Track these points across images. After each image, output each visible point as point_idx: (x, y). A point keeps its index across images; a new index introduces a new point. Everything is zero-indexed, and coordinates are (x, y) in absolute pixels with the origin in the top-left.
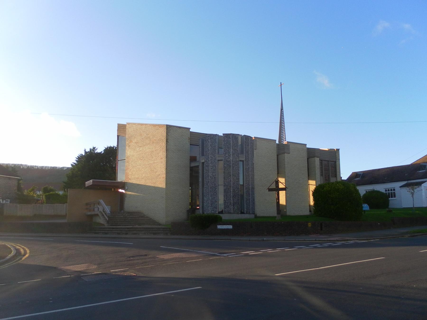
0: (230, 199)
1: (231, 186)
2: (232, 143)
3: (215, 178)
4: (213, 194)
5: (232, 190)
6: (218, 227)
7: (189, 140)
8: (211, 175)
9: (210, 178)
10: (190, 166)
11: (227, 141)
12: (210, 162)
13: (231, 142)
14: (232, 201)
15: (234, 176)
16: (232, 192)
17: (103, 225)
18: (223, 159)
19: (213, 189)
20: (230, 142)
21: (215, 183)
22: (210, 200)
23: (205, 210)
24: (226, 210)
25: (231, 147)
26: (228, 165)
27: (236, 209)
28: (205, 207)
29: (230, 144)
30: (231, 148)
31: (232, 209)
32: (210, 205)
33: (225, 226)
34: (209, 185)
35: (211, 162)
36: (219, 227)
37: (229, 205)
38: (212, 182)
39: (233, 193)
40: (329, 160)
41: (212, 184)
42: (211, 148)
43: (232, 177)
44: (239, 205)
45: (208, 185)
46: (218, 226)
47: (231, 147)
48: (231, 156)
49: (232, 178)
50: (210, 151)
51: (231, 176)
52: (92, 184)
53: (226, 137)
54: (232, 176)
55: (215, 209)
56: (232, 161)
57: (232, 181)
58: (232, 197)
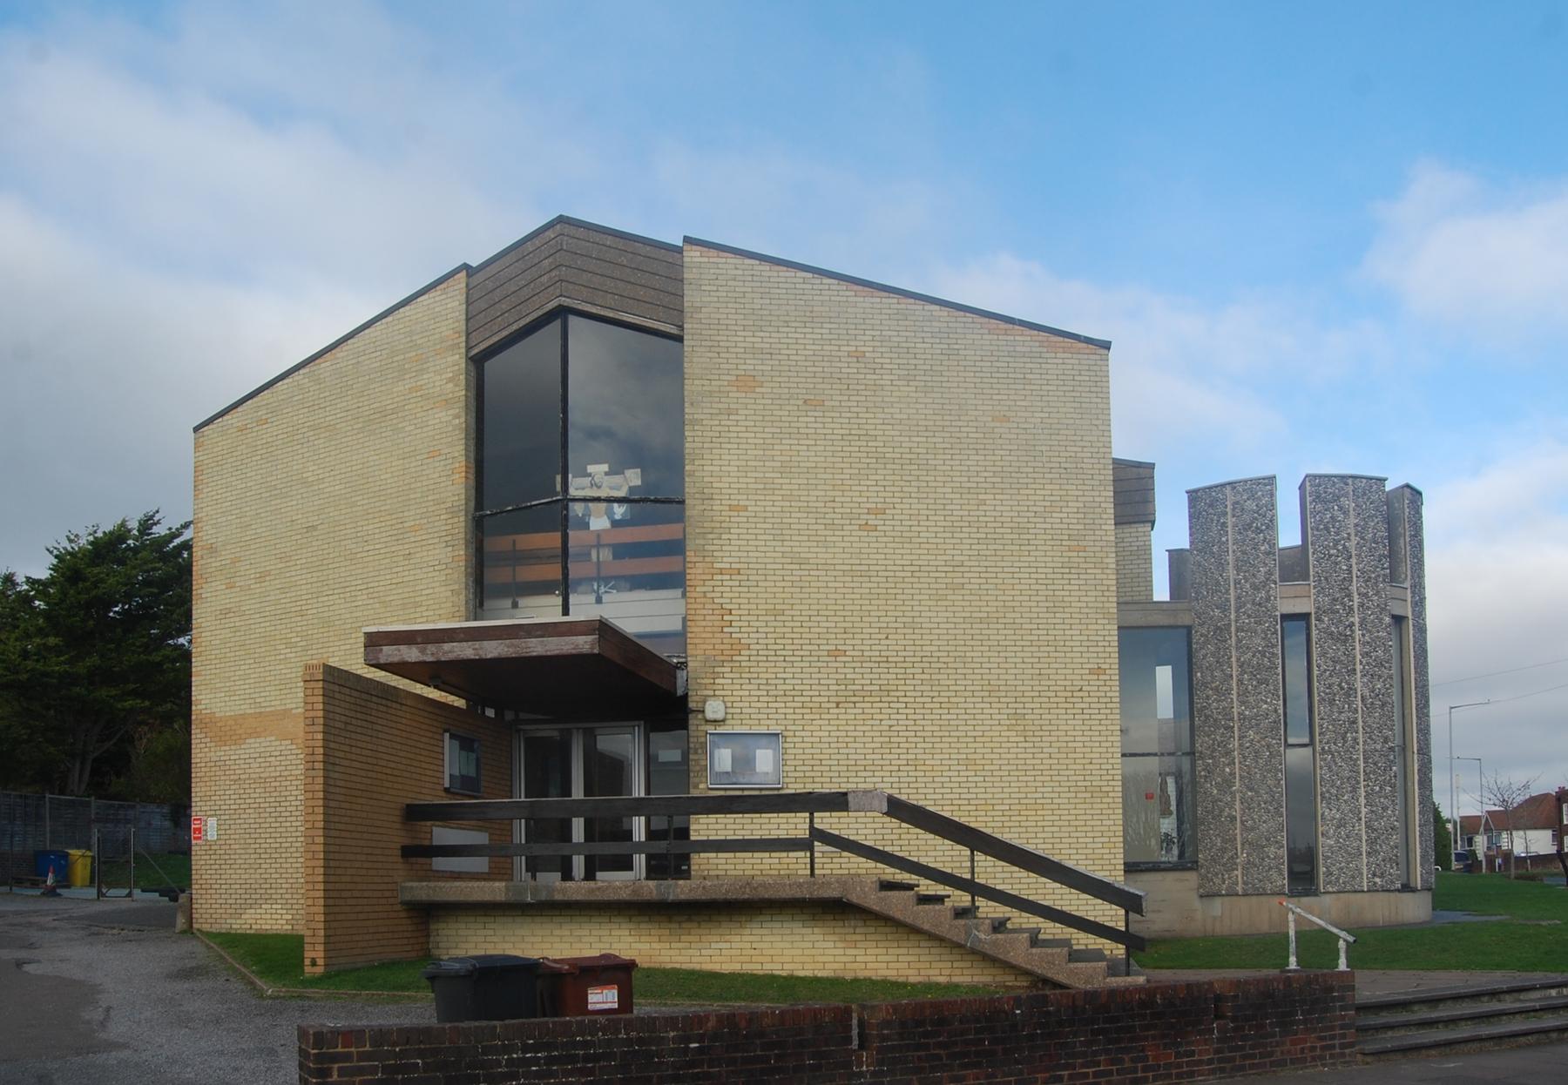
3: (1383, 705)
4: (1378, 788)
12: (1356, 620)
19: (1375, 764)
28: (1329, 858)
32: (1364, 848)
34: (1355, 740)
35: (1363, 622)
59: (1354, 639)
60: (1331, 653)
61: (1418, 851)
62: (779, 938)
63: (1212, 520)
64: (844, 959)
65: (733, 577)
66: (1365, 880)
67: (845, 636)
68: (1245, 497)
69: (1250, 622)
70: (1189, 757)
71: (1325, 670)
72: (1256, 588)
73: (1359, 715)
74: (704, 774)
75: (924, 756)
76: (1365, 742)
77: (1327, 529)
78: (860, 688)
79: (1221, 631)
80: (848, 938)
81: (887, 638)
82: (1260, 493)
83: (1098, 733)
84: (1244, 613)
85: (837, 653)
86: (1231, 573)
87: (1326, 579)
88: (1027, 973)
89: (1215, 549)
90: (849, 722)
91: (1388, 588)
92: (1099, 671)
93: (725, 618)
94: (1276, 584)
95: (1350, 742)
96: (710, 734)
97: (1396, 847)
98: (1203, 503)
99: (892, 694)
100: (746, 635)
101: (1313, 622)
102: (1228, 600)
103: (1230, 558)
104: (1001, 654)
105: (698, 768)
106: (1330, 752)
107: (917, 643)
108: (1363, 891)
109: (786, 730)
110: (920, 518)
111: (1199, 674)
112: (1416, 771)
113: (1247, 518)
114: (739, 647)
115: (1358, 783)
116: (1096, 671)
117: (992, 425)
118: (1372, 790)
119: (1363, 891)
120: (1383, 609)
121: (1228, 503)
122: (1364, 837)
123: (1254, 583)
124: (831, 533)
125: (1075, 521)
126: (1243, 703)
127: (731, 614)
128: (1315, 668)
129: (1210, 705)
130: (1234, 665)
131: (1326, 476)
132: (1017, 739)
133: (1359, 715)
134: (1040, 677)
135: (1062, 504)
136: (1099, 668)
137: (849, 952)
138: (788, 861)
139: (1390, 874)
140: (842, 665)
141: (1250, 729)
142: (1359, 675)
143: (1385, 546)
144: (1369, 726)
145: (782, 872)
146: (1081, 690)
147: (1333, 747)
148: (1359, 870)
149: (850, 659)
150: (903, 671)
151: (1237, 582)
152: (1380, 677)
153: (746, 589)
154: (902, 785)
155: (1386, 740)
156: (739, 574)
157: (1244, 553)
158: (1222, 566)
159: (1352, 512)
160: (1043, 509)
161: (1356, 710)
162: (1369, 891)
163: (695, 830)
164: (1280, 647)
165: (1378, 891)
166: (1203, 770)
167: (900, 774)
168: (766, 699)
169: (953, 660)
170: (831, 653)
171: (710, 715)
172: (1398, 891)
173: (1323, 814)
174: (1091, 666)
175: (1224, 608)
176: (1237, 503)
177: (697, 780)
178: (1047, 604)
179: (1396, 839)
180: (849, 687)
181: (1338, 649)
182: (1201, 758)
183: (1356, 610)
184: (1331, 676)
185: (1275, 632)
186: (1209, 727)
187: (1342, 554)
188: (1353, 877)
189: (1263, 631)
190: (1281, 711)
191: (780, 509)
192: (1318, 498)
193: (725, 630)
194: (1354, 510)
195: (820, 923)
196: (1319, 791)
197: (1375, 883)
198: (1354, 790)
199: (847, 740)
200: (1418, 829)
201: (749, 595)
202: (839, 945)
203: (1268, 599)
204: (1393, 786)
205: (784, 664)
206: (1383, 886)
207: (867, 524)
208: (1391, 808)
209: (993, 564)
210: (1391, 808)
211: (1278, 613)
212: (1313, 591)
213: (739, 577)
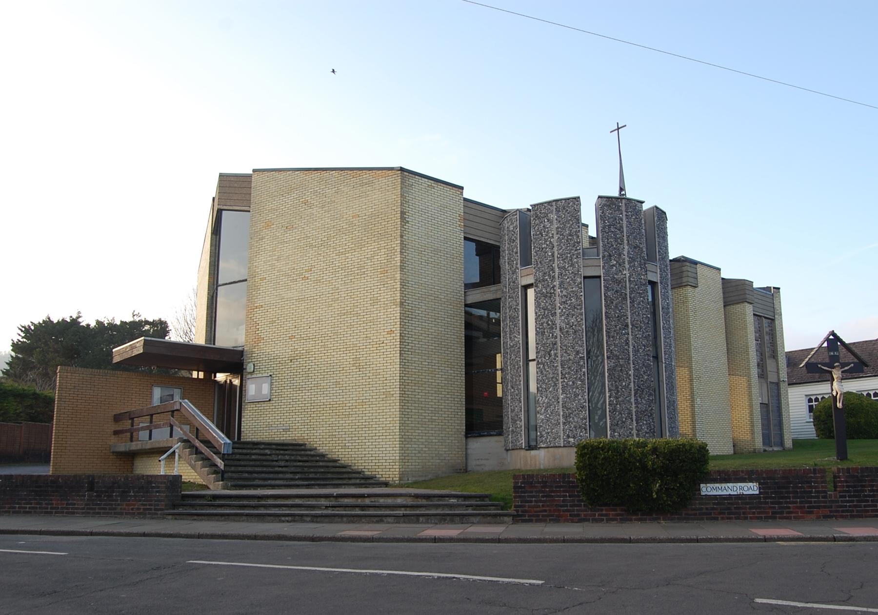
0: (627, 399)
1: (629, 359)
2: (627, 227)
5: (631, 372)
6: (704, 489)
7: (462, 224)
9: (557, 332)
10: (465, 300)
11: (612, 219)
12: (557, 283)
13: (625, 222)
14: (634, 405)
15: (637, 327)
16: (632, 378)
17: (206, 487)
18: (601, 272)
19: (569, 368)
20: (619, 223)
21: (577, 348)
22: (561, 403)
23: (542, 436)
24: (616, 434)
25: (625, 238)
26: (616, 291)
27: (646, 433)
28: (541, 426)
29: (622, 227)
30: (626, 242)
31: (634, 432)
32: (562, 420)
33: (730, 485)
34: (556, 355)
35: (561, 284)
36: (708, 489)
37: (624, 420)
38: (565, 346)
39: (634, 382)
40: (761, 314)
41: (566, 352)
43: (630, 330)
44: (653, 419)
45: (550, 356)
46: (702, 485)
47: (625, 238)
48: (627, 266)
49: (632, 332)
50: (555, 249)
51: (627, 326)
52: (142, 352)
53: (609, 206)
54: (630, 326)
56: (630, 281)
57: (631, 343)
58: (633, 392)
59: (555, 294)
73: (558, 339)
75: (321, 382)
77: (541, 234)
87: (541, 262)
97: (585, 419)
108: (561, 447)
115: (558, 380)
118: (567, 384)
119: (561, 447)
131: (540, 204)
133: (558, 339)
139: (581, 436)
142: (558, 315)
146: (383, 343)
147: (543, 359)
152: (573, 315)
155: (578, 353)
165: (571, 446)
167: (312, 391)
174: (388, 330)
178: (371, 302)
181: (547, 302)
184: (542, 318)
194: (557, 219)
198: (556, 385)
204: (582, 381)
206: (574, 443)
211: (520, 286)
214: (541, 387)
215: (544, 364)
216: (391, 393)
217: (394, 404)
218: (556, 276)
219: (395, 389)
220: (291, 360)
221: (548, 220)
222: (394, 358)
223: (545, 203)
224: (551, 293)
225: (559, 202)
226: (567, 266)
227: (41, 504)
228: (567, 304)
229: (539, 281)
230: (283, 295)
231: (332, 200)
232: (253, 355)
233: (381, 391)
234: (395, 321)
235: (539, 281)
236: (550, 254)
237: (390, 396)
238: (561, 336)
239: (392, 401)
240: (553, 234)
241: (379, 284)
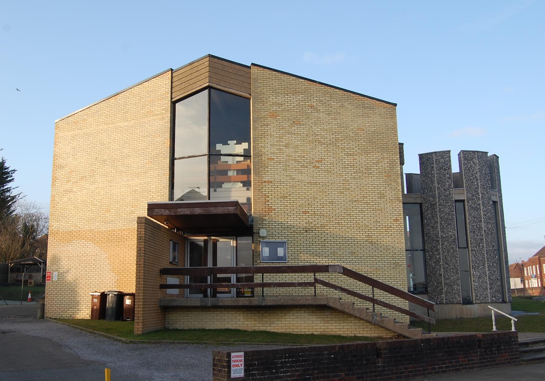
4: (492, 264)
8: (486, 229)
12: (481, 202)
19: (490, 255)
28: (476, 290)
32: (488, 286)
34: (483, 246)
38: (487, 241)
42: (480, 176)
50: (479, 181)
55: (498, 294)
59: (480, 209)
60: (473, 215)
61: (506, 288)
62: (300, 320)
63: (428, 165)
64: (324, 327)
65: (269, 184)
66: (489, 299)
67: (308, 206)
68: (440, 158)
69: (443, 203)
70: (422, 252)
71: (471, 221)
72: (445, 190)
74: (259, 257)
76: (486, 247)
78: (314, 225)
79: (433, 205)
80: (325, 319)
81: (323, 207)
82: (445, 157)
83: (397, 243)
84: (441, 199)
85: (305, 212)
86: (436, 184)
87: (470, 188)
88: (395, 332)
89: (430, 176)
90: (310, 238)
91: (491, 191)
92: (396, 220)
93: (266, 199)
94: (452, 189)
95: (481, 247)
96: (262, 242)
97: (499, 286)
98: (425, 159)
99: (325, 227)
100: (274, 205)
101: (466, 203)
102: (435, 194)
103: (435, 179)
104: (363, 214)
105: (257, 255)
106: (474, 250)
107: (334, 209)
108: (489, 303)
109: (288, 241)
110: (334, 164)
111: (425, 221)
112: (504, 258)
113: (441, 165)
114: (271, 210)
116: (396, 220)
117: (358, 132)
118: (490, 265)
119: (489, 303)
120: (489, 199)
121: (434, 159)
122: (488, 282)
123: (444, 188)
124: (303, 169)
125: (387, 166)
126: (442, 232)
127: (268, 198)
128: (468, 220)
129: (430, 232)
130: (439, 218)
132: (369, 245)
134: (376, 222)
135: (382, 160)
136: (397, 219)
137: (326, 325)
138: (289, 290)
139: (498, 297)
140: (308, 217)
141: (445, 241)
143: (489, 176)
144: (487, 241)
145: (287, 294)
146: (391, 227)
147: (475, 248)
148: (487, 294)
149: (310, 215)
150: (329, 219)
151: (438, 188)
153: (274, 189)
154: (329, 262)
156: (271, 183)
157: (440, 177)
158: (432, 182)
159: (477, 164)
160: (376, 162)
161: (483, 235)
162: (491, 303)
163: (256, 278)
164: (455, 212)
165: (494, 303)
166: (428, 256)
167: (329, 257)
168: (281, 229)
169: (346, 215)
170: (304, 212)
171: (261, 235)
172: (501, 303)
173: (473, 274)
174: (394, 218)
175: (434, 197)
176: (437, 160)
177: (256, 259)
178: (378, 196)
179: (499, 283)
180: (310, 225)
182: (428, 252)
183: (481, 199)
185: (453, 206)
186: (430, 240)
187: (475, 179)
188: (485, 297)
189: (448, 206)
190: (456, 235)
191: (285, 160)
192: (465, 159)
193: (266, 203)
195: (315, 314)
196: (471, 265)
197: (493, 300)
198: (484, 265)
199: (310, 244)
200: (506, 279)
201: (275, 191)
202: (322, 322)
203: (450, 194)
205: (287, 216)
207: (315, 166)
208: (497, 272)
209: (359, 181)
210: (497, 272)
211: (454, 200)
212: (465, 192)
213: (271, 184)
214: (474, 265)
215: (475, 252)
216: (400, 264)
217: (402, 272)
218: (480, 198)
219: (402, 261)
220: (306, 231)
221: (473, 163)
222: (401, 239)
223: (471, 151)
224: (478, 208)
225: (478, 153)
226: (485, 193)
227: (452, 363)
228: (486, 216)
229: (470, 199)
230: (293, 177)
231: (338, 111)
232: (264, 222)
233: (391, 262)
234: (399, 212)
235: (470, 199)
236: (476, 184)
237: (399, 266)
238: (485, 235)
239: (401, 270)
240: (476, 172)
241: (385, 184)
